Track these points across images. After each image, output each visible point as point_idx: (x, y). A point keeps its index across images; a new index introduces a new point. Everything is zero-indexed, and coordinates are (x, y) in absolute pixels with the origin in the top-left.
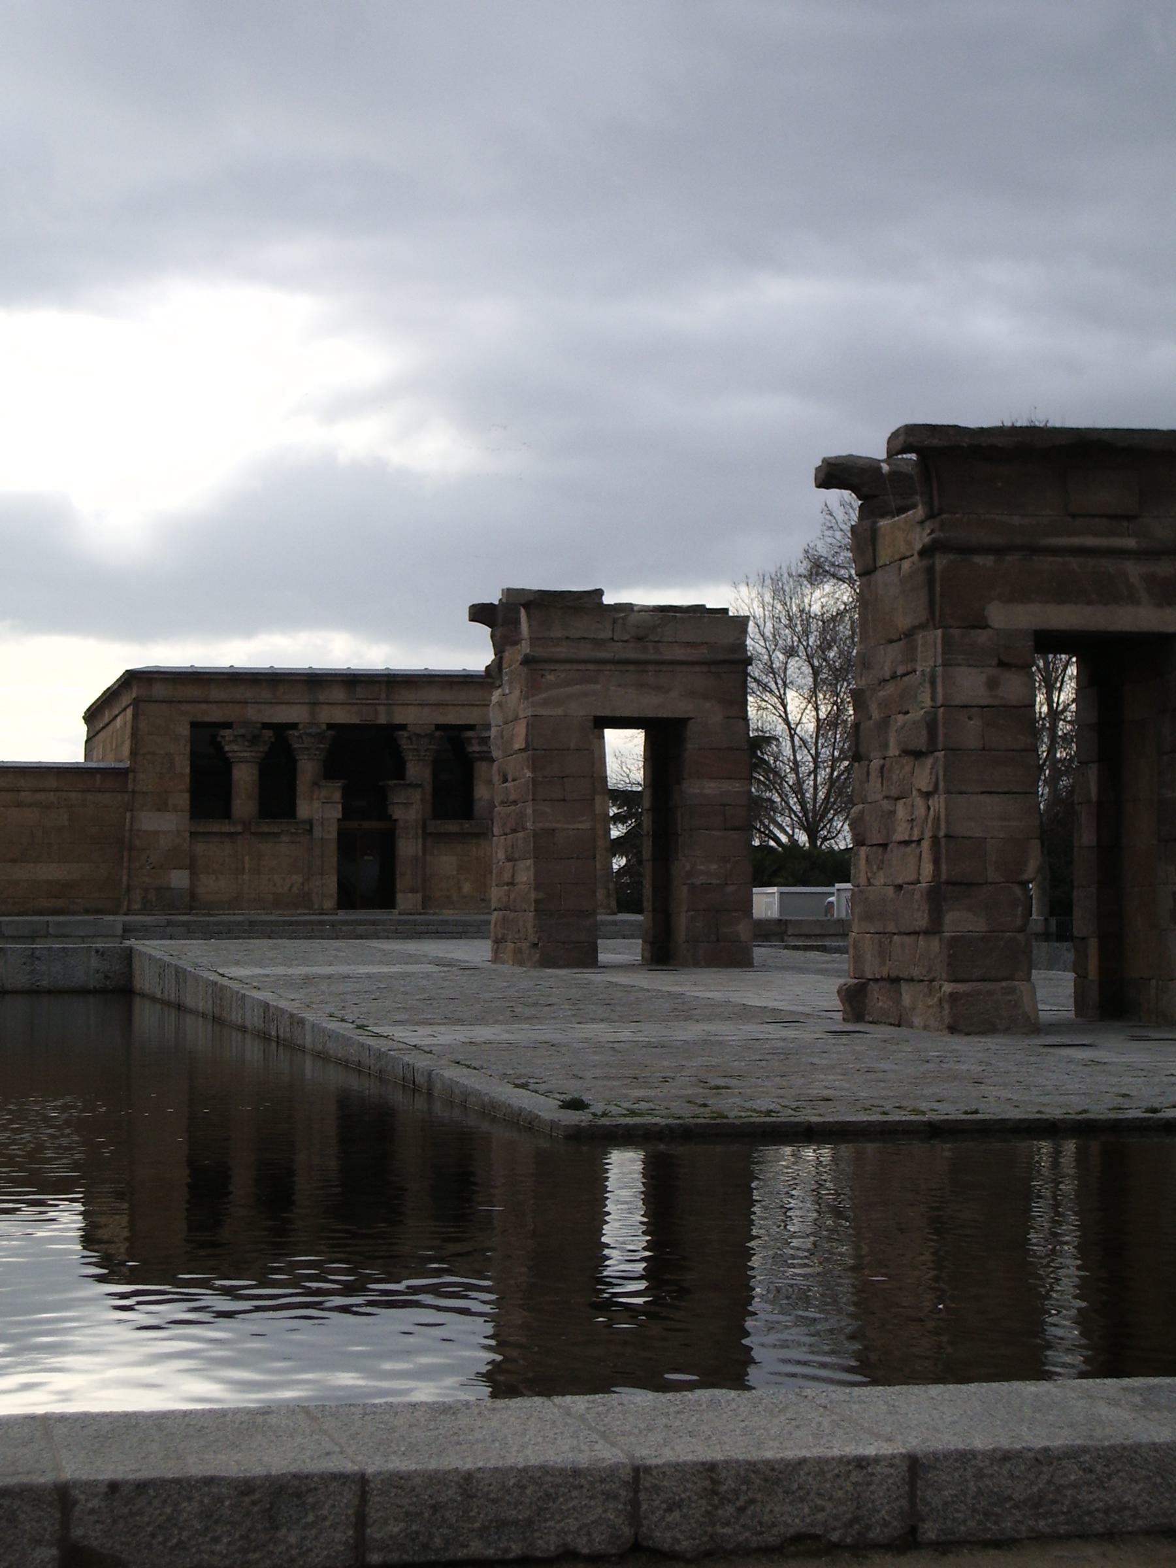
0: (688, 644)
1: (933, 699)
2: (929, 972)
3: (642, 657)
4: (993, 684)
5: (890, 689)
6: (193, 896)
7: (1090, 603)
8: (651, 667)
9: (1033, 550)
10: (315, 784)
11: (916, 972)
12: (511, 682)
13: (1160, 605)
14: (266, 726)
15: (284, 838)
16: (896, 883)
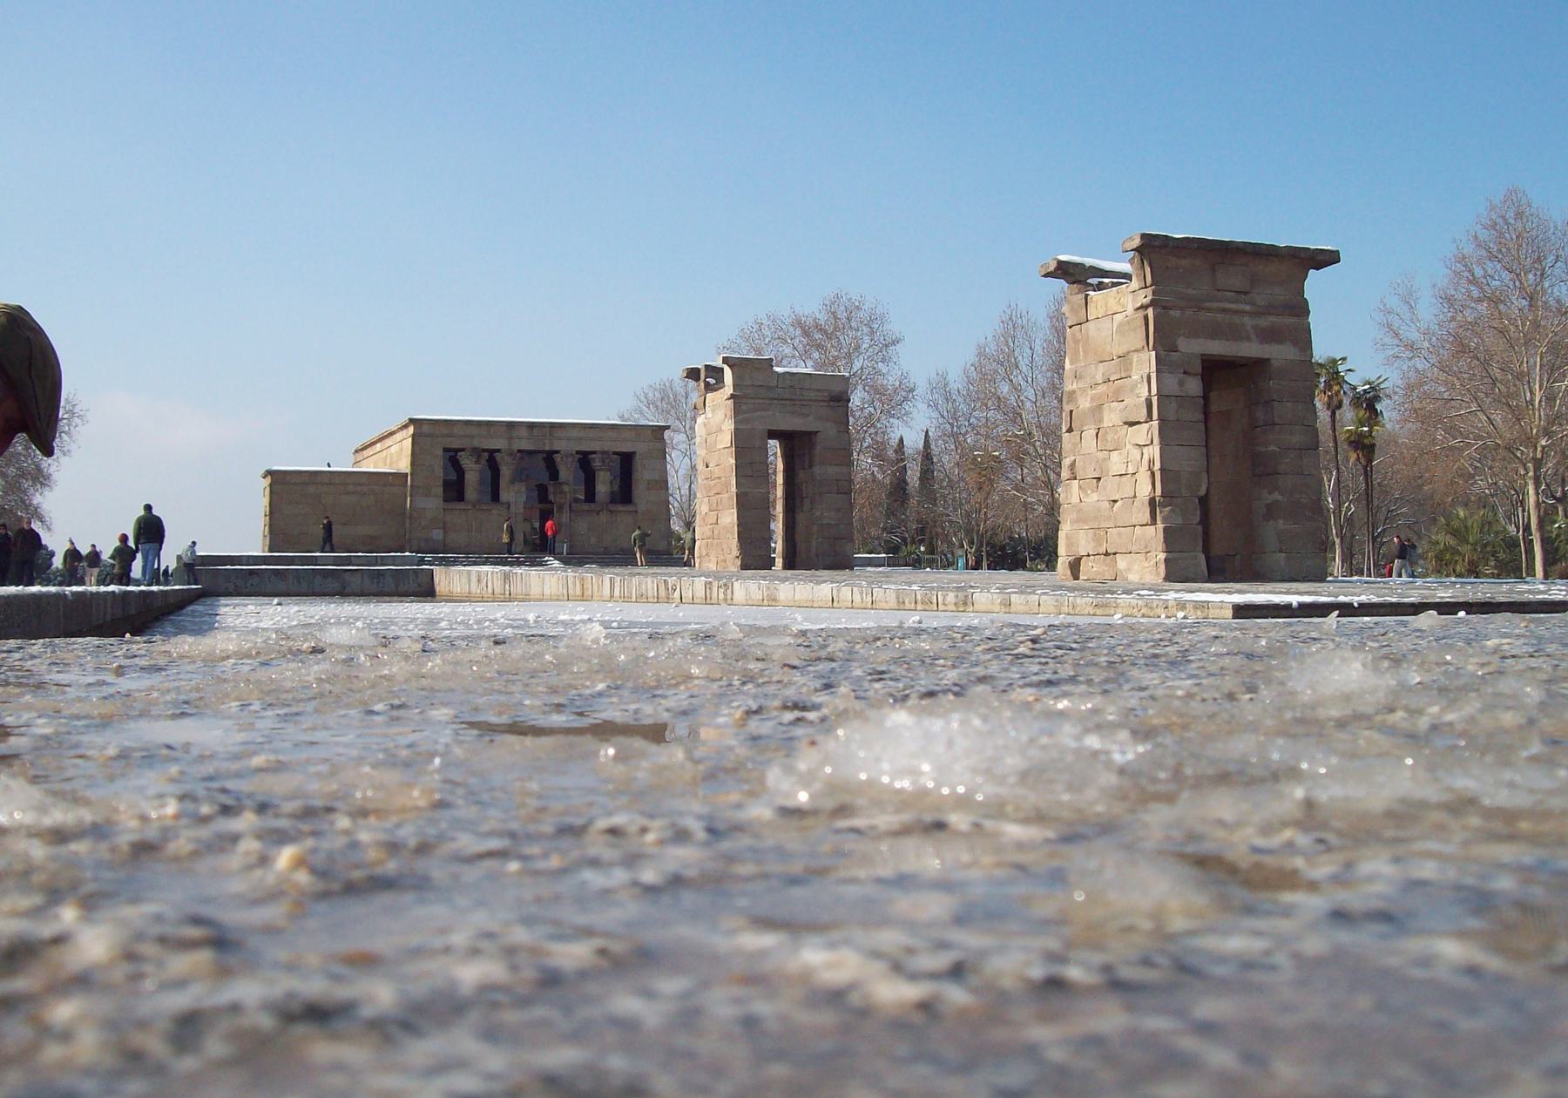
0: (818, 390)
1: (1150, 391)
2: (1146, 547)
3: (794, 397)
4: (1181, 383)
5: (1102, 388)
6: (444, 545)
7: (1227, 340)
8: (797, 402)
9: (1200, 309)
10: (512, 481)
11: (1134, 549)
12: (713, 411)
13: (1261, 343)
14: (484, 450)
15: (495, 512)
16: (1112, 499)
